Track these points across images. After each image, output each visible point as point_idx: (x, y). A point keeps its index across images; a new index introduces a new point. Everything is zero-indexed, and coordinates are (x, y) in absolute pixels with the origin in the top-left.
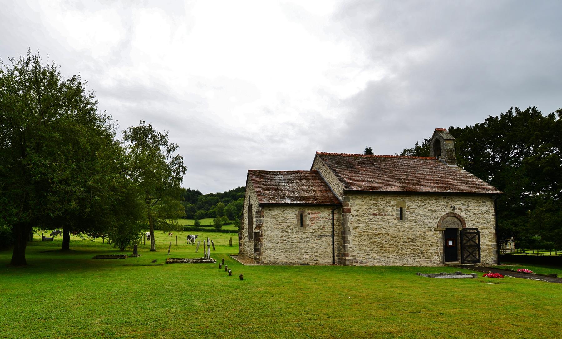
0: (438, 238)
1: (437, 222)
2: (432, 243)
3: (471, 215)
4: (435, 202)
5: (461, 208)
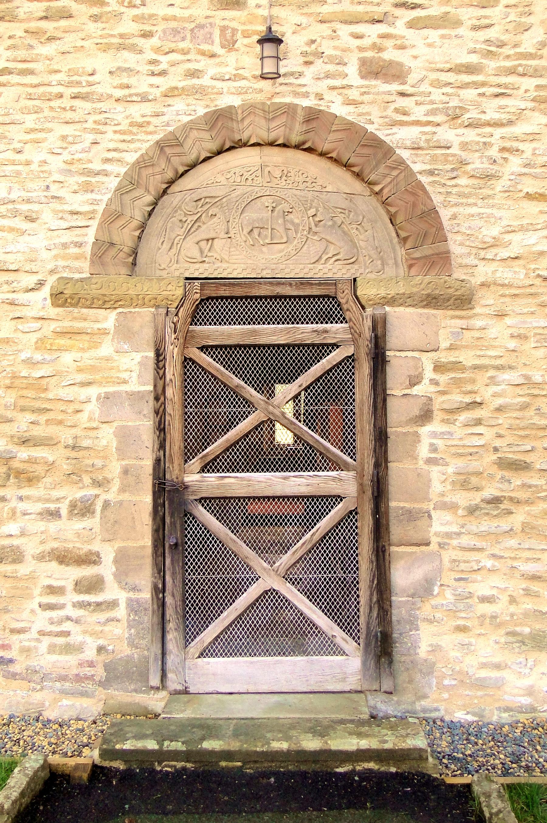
0: (93, 392)
1: (91, 215)
2: (25, 442)
3: (519, 129)
5: (391, 54)
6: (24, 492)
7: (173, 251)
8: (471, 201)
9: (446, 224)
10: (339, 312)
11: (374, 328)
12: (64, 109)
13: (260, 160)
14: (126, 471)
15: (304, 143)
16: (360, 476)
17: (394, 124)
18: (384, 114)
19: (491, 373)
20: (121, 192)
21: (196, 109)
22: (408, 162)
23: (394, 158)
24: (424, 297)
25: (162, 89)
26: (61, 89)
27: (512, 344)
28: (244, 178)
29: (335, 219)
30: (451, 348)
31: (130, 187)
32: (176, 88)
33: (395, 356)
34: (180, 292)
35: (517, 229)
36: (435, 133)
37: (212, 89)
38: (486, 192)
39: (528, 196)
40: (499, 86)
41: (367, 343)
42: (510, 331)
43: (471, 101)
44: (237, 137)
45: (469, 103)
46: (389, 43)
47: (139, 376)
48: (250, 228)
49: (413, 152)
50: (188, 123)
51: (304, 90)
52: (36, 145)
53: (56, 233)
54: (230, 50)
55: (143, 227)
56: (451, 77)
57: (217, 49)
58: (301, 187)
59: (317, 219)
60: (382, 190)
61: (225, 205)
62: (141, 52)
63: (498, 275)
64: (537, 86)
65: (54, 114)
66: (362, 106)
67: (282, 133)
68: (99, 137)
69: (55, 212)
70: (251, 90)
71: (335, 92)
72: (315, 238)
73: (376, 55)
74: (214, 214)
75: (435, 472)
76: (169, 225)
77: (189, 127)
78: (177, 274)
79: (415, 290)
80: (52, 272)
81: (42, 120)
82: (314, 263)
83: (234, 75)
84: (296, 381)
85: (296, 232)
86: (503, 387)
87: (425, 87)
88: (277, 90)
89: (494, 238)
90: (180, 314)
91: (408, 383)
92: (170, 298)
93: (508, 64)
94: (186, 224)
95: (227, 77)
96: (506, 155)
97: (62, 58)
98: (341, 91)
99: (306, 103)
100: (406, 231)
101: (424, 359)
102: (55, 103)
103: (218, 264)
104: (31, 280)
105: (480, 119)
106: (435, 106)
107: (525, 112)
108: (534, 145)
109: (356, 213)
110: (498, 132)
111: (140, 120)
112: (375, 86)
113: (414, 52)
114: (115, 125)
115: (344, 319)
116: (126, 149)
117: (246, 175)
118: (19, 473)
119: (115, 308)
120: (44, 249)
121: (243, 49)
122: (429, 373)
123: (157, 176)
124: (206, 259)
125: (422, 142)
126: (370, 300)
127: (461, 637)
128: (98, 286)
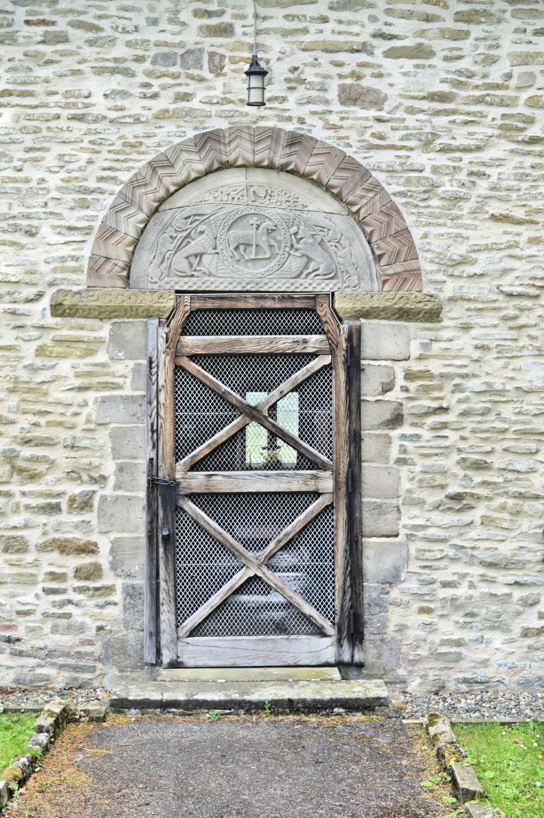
0: (91, 396)
2: (27, 442)
4: (73, 24)
5: (367, 82)
6: (27, 488)
7: (165, 265)
8: (441, 221)
9: (418, 242)
10: (318, 324)
11: (349, 339)
12: (61, 130)
13: (245, 181)
14: (121, 469)
15: (288, 164)
16: (336, 474)
17: (371, 147)
18: (363, 138)
19: (457, 381)
20: (116, 209)
21: (186, 130)
22: (384, 185)
23: (370, 181)
24: (396, 311)
25: (154, 111)
26: (58, 111)
27: (476, 354)
28: (230, 197)
29: (315, 237)
30: (421, 358)
31: (124, 205)
32: (167, 111)
33: (369, 365)
34: (170, 304)
35: (482, 249)
36: (408, 157)
37: (201, 112)
38: (455, 212)
39: (494, 218)
40: (468, 114)
41: (344, 352)
42: (475, 342)
43: (442, 128)
44: (224, 159)
45: (441, 129)
46: (367, 72)
47: (133, 382)
48: (236, 244)
49: (388, 175)
50: (179, 144)
51: (287, 114)
52: (35, 163)
53: (54, 247)
54: (218, 75)
55: (136, 243)
56: (425, 105)
57: (205, 73)
58: (285, 205)
59: (299, 236)
60: (358, 211)
61: (213, 222)
62: (133, 75)
63: (465, 290)
64: (504, 116)
65: (52, 134)
66: (342, 130)
67: (267, 156)
68: (94, 156)
69: (54, 227)
70: (237, 114)
71: (316, 118)
72: (297, 254)
73: (355, 83)
74: (202, 230)
75: (404, 471)
76: (161, 241)
77: (180, 149)
78: (168, 287)
79: (388, 304)
80: (51, 284)
81: (40, 139)
82: (295, 278)
83: (222, 99)
84: (278, 388)
85: (279, 249)
86: (467, 394)
87: (400, 114)
88: (262, 114)
89: (462, 256)
90: (171, 325)
91: (380, 390)
92: (162, 309)
93: (477, 93)
94: (176, 240)
95: (215, 101)
96: (473, 179)
97: (59, 80)
98: (322, 116)
99: (289, 127)
100: (381, 249)
101: (396, 368)
102: (53, 124)
103: (206, 278)
104: (31, 292)
105: (450, 145)
106: (409, 132)
107: (492, 139)
108: (501, 169)
109: (334, 231)
110: (467, 157)
111: (133, 140)
112: (354, 112)
113: (390, 80)
114: (109, 145)
115: (323, 330)
116: (119, 167)
117: (233, 194)
118: (21, 471)
119: (110, 318)
120: (42, 263)
121: (230, 74)
122: (400, 382)
123: (149, 195)
124: (195, 273)
125: (396, 166)
126: (347, 313)
127: (426, 618)
128: (95, 298)
